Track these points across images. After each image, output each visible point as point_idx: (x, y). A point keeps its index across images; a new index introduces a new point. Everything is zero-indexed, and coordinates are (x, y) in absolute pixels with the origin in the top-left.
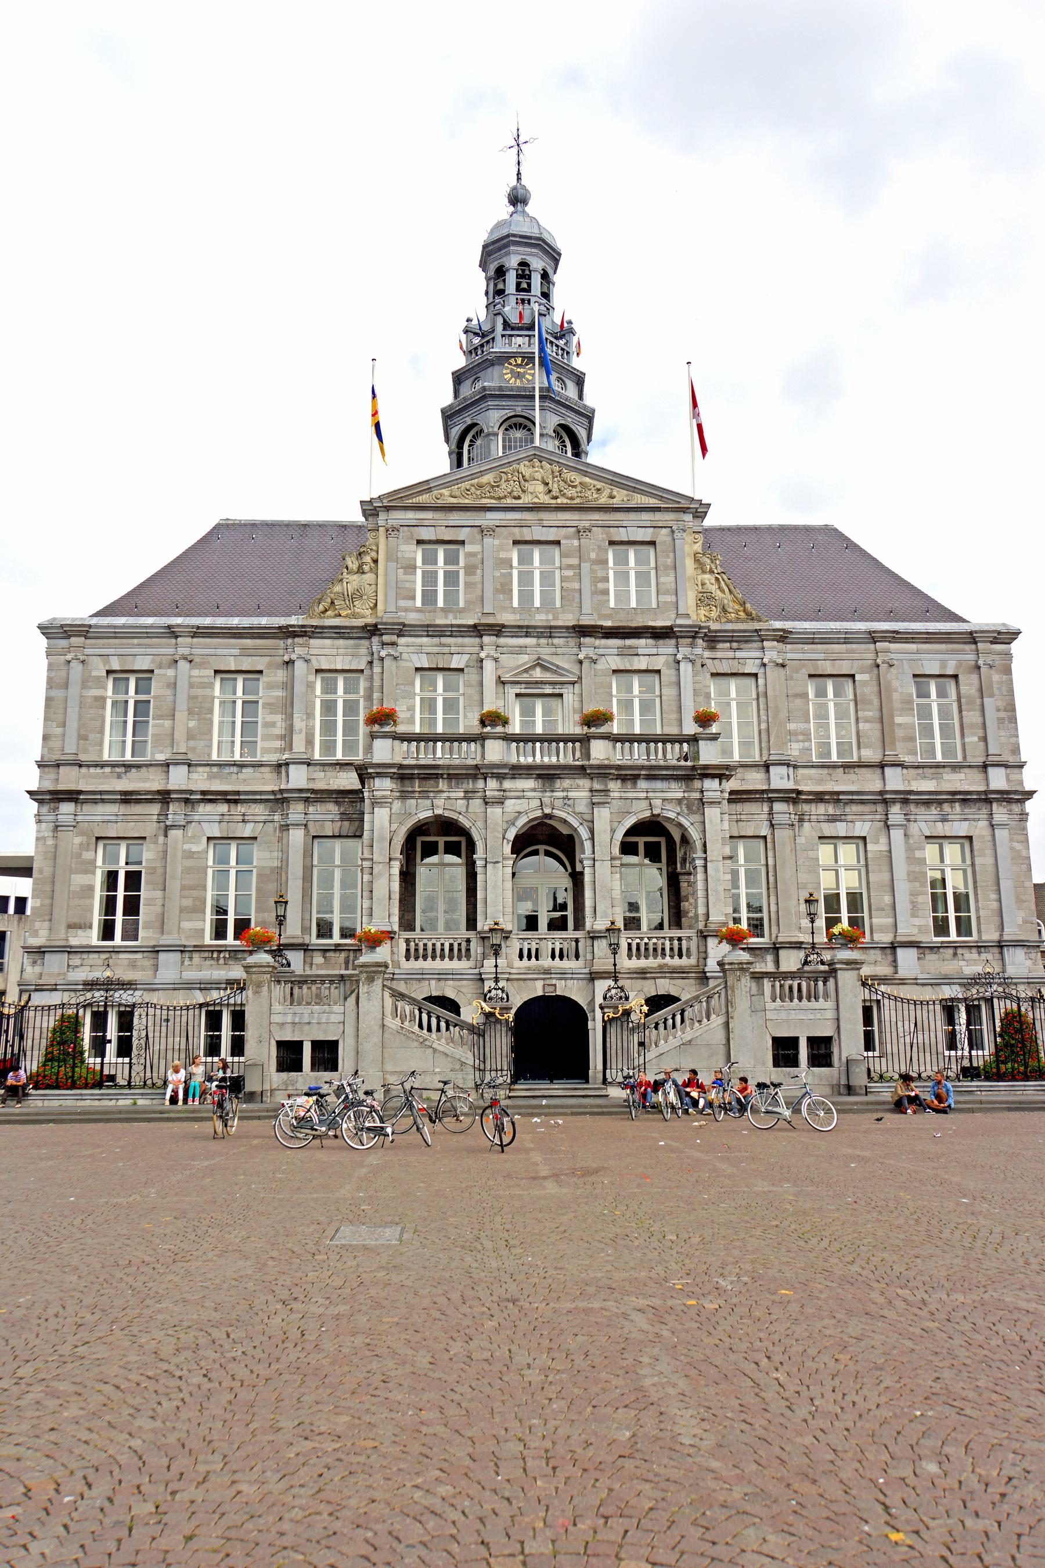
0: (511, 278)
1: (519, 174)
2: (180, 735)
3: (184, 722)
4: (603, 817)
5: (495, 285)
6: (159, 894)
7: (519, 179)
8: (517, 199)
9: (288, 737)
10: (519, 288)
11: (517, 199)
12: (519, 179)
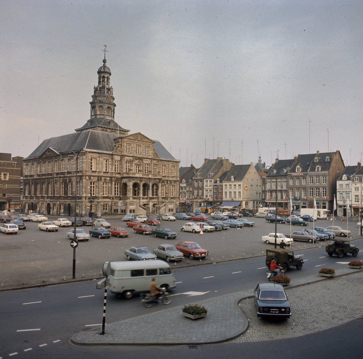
0: (106, 79)
1: (105, 57)
2: (100, 168)
3: (100, 166)
4: (151, 183)
5: (103, 79)
6: (98, 189)
7: (105, 58)
8: (104, 61)
9: (112, 169)
10: (107, 82)
11: (104, 61)
12: (105, 58)
